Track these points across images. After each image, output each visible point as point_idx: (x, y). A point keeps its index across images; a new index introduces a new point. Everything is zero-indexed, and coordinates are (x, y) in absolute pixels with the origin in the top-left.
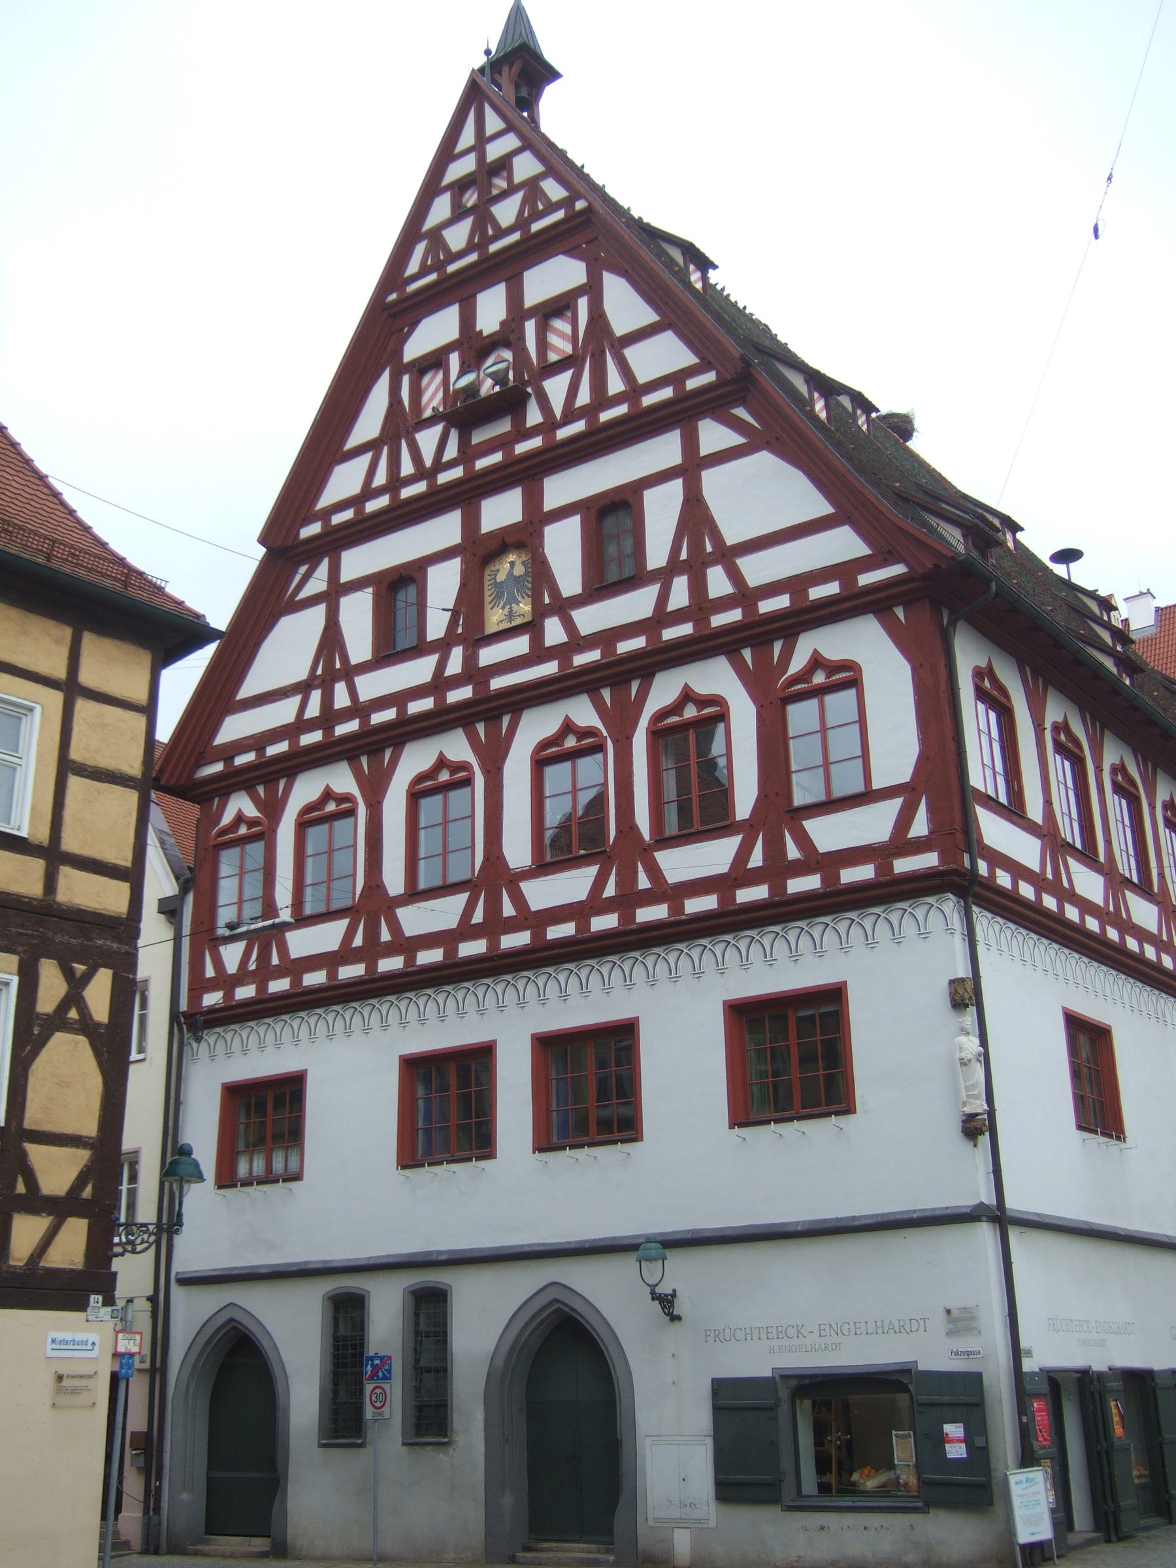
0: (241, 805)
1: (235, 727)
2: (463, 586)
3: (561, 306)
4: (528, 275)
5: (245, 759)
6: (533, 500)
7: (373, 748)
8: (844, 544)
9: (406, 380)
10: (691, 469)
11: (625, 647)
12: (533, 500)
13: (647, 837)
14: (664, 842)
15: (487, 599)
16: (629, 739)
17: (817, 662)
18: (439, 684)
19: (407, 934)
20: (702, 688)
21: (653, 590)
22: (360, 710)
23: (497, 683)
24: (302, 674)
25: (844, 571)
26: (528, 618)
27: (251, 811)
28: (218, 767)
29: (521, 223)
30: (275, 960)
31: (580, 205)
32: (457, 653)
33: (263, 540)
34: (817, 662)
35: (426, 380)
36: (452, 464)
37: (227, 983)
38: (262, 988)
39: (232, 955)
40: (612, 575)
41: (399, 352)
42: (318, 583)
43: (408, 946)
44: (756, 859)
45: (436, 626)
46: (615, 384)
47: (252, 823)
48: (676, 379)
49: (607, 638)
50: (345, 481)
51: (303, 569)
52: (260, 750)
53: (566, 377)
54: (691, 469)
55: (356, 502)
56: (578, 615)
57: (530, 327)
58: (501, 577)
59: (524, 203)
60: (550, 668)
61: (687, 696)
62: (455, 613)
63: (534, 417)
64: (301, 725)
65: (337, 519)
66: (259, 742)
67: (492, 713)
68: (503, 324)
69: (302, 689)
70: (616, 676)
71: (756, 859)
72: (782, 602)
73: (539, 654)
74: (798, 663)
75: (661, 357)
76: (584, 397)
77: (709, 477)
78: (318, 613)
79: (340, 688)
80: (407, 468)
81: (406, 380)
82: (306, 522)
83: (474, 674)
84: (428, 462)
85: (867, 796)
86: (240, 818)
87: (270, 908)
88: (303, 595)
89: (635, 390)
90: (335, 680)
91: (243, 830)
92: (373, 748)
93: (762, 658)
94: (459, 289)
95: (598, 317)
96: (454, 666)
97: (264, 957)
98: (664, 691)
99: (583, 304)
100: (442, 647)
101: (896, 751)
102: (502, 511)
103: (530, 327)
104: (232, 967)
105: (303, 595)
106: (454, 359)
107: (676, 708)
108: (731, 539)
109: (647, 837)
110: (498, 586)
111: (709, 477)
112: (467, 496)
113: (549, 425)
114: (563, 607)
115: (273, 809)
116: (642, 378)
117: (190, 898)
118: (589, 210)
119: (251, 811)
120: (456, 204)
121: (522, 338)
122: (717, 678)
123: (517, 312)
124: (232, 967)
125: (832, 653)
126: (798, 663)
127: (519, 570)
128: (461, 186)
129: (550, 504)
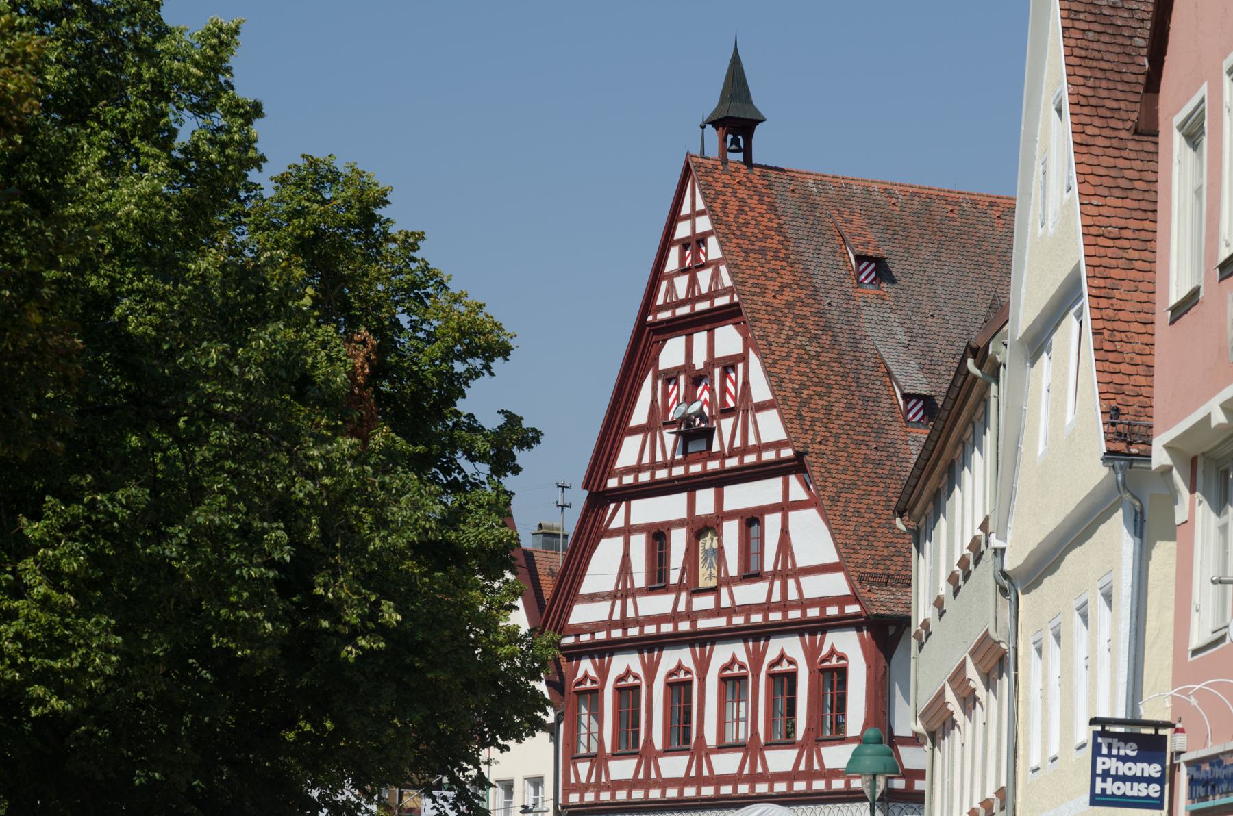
0: (586, 666)
1: (581, 614)
2: (687, 550)
3: (729, 365)
4: (717, 330)
5: (585, 638)
6: (719, 500)
7: (650, 646)
8: (837, 584)
9: (660, 382)
10: (786, 507)
11: (757, 618)
12: (719, 500)
13: (762, 740)
14: (770, 745)
15: (701, 560)
16: (758, 676)
17: (832, 652)
18: (674, 617)
19: (664, 776)
20: (789, 653)
21: (764, 585)
22: (640, 622)
23: (703, 624)
24: (612, 588)
25: (840, 601)
26: (713, 583)
27: (592, 673)
28: (570, 640)
29: (710, 296)
30: (603, 780)
31: (736, 299)
32: (683, 595)
33: (585, 487)
34: (832, 652)
35: (671, 387)
36: (679, 463)
37: (582, 788)
38: (597, 796)
39: (583, 767)
40: (754, 568)
41: (656, 359)
42: (618, 522)
43: (665, 783)
44: (802, 767)
45: (674, 578)
46: (752, 441)
47: (593, 681)
48: (777, 445)
49: (747, 610)
50: (629, 451)
51: (612, 506)
52: (593, 633)
53: (731, 420)
54: (786, 507)
55: (637, 469)
56: (736, 589)
57: (717, 371)
58: (707, 547)
59: (712, 279)
60: (721, 622)
61: (782, 656)
62: (683, 569)
63: (716, 447)
64: (609, 625)
65: (628, 480)
66: (594, 627)
67: (702, 640)
68: (705, 363)
69: (612, 596)
70: (757, 635)
71: (802, 767)
72: (813, 612)
73: (717, 612)
74: (825, 651)
75: (770, 426)
76: (738, 443)
77: (793, 515)
78: (619, 541)
79: (630, 601)
80: (659, 458)
81: (660, 382)
82: (611, 476)
83: (692, 616)
84: (669, 458)
85: (844, 740)
86: (586, 676)
87: (601, 742)
88: (612, 526)
89: (760, 448)
90: (627, 597)
91: (589, 684)
92: (650, 646)
93: (813, 642)
94: (685, 326)
95: (746, 383)
96: (682, 608)
97: (598, 776)
98: (774, 647)
99: (740, 366)
100: (678, 588)
101: (856, 718)
102: (705, 501)
103: (717, 371)
104: (583, 780)
105: (612, 526)
106: (682, 378)
107: (778, 662)
108: (801, 562)
109: (762, 740)
110: (705, 551)
111: (793, 515)
112: (689, 485)
113: (722, 456)
114: (729, 582)
115: (603, 672)
116: (764, 440)
117: (562, 726)
118: (737, 304)
119: (592, 673)
120: (682, 259)
121: (712, 381)
122: (793, 646)
123: (712, 362)
124: (583, 780)
125: (839, 649)
126: (825, 651)
127: (715, 545)
128: (685, 244)
129: (728, 506)
